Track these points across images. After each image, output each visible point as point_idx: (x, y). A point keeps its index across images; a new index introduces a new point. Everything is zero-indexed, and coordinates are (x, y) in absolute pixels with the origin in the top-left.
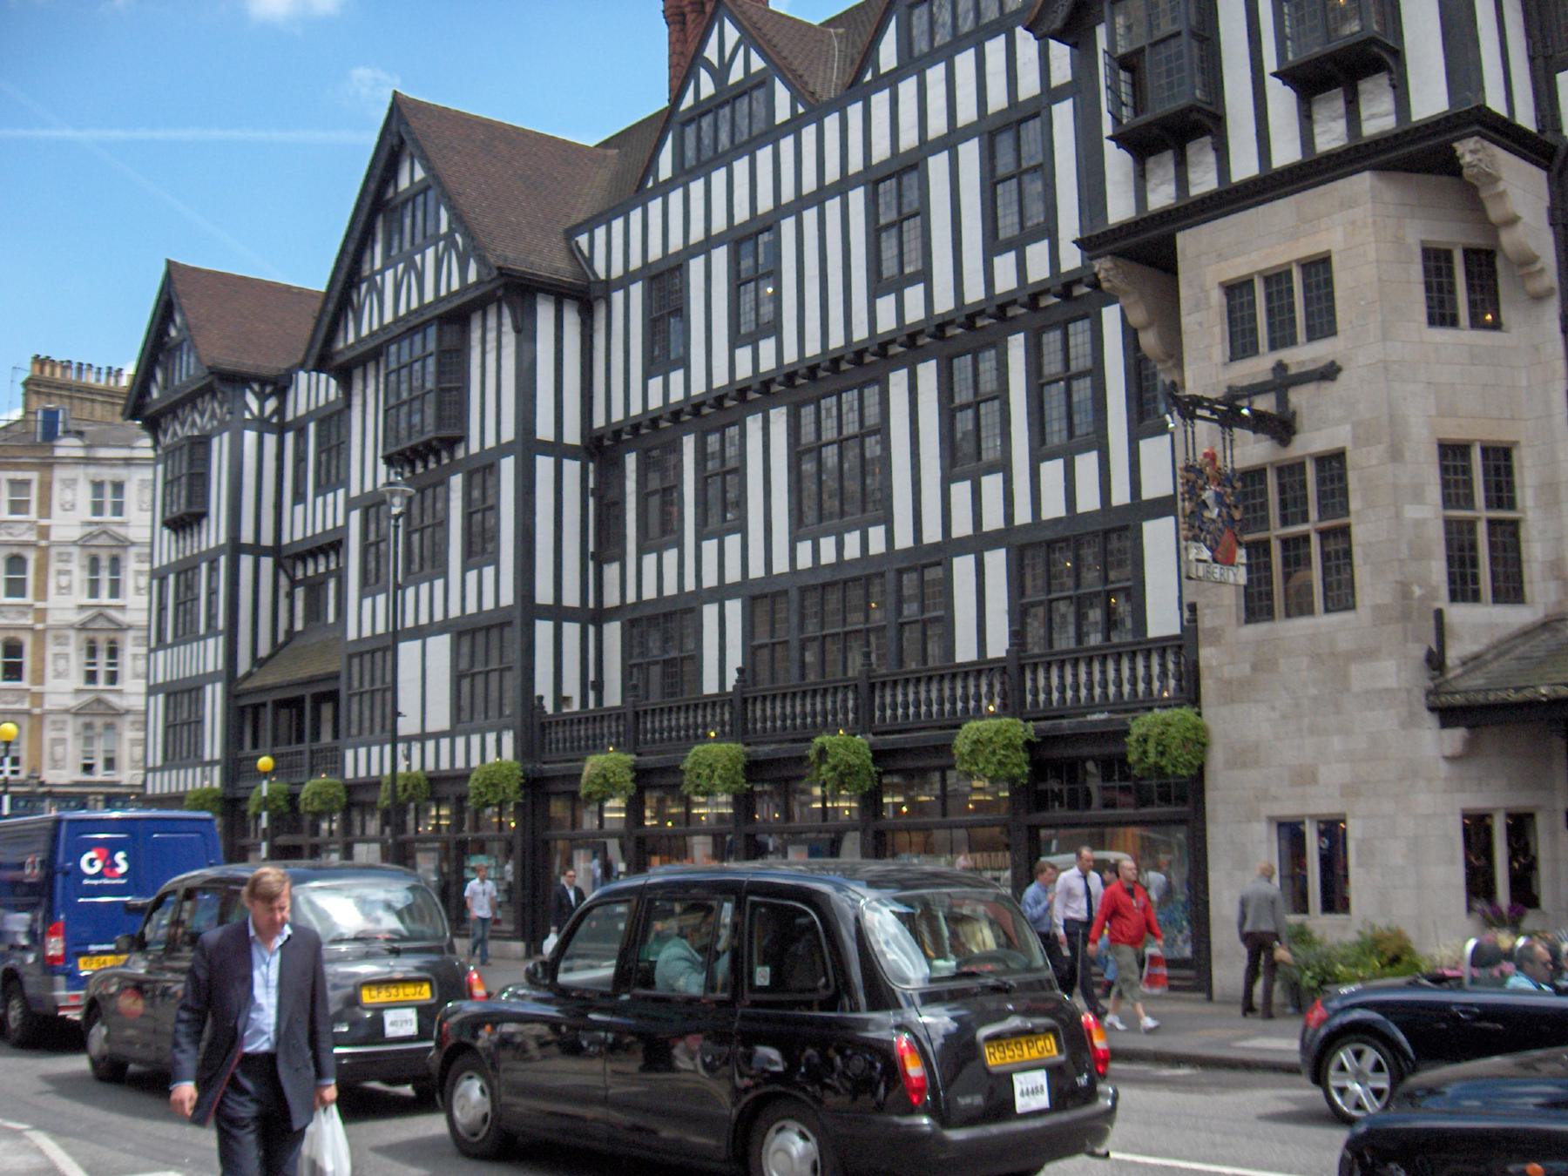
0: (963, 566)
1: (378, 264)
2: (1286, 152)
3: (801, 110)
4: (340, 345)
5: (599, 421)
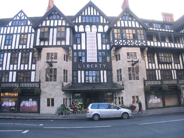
0: (11, 73)
2: (55, 44)
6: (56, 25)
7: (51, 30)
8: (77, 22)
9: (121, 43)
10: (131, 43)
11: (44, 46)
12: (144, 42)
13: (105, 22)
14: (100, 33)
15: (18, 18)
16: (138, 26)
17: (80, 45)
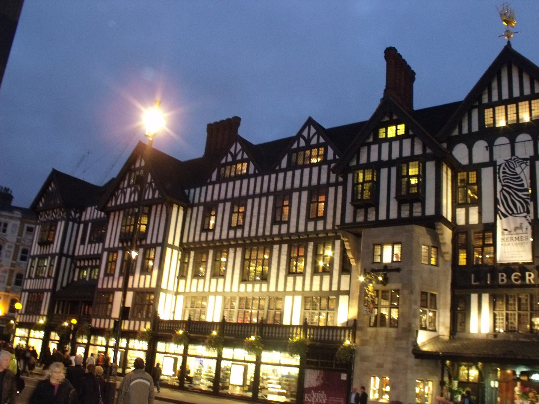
1: (125, 185)
2: (393, 215)
4: (109, 205)
5: (185, 241)
6: (395, 155)
7: (384, 172)
8: (465, 131)
11: (367, 224)
15: (302, 143)
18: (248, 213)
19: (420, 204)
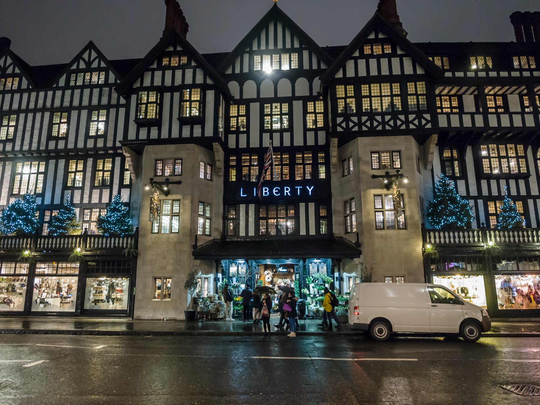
2: (175, 134)
3: (31, 87)
6: (178, 82)
8: (237, 71)
9: (379, 124)
10: (384, 123)
11: (150, 142)
12: (428, 116)
13: (315, 67)
14: (299, 98)
15: (82, 65)
16: (409, 70)
17: (245, 135)
18: (20, 128)
19: (200, 126)
